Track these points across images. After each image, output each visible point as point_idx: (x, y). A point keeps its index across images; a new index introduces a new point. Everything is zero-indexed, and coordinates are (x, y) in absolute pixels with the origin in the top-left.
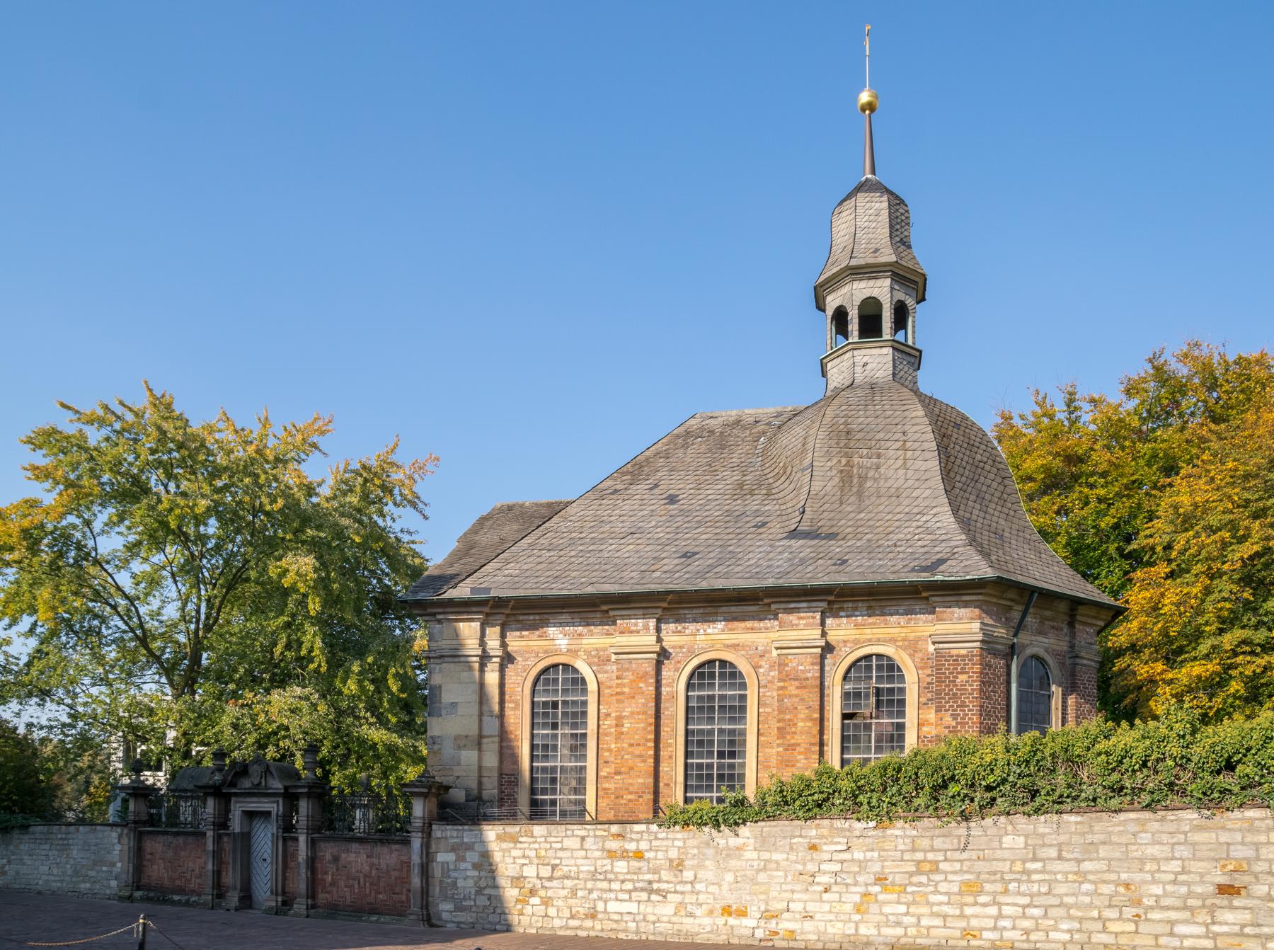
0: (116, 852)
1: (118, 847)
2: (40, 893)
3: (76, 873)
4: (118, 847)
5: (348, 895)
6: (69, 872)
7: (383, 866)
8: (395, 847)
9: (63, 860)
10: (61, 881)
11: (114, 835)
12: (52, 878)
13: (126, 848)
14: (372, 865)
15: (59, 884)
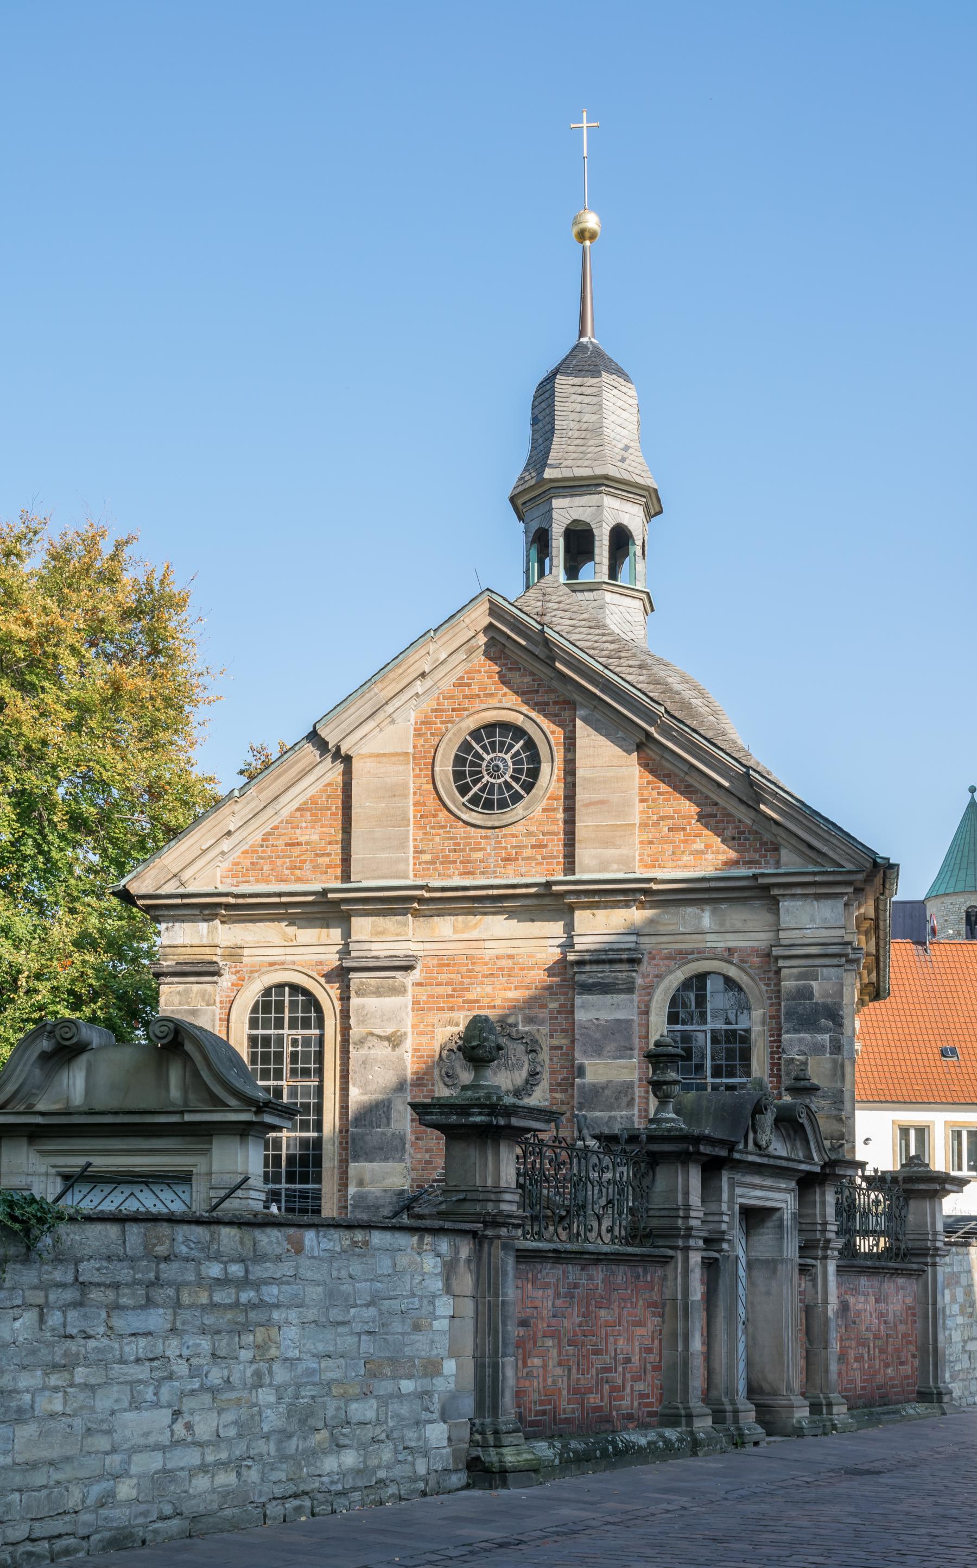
0: (441, 1325)
1: (445, 1306)
2: (120, 1541)
3: (303, 1418)
4: (445, 1306)
5: (857, 1373)
6: (272, 1420)
7: (891, 1318)
8: (901, 1281)
9: (242, 1371)
10: (237, 1465)
11: (430, 1264)
12: (193, 1458)
13: (468, 1307)
14: (881, 1315)
15: (227, 1479)
